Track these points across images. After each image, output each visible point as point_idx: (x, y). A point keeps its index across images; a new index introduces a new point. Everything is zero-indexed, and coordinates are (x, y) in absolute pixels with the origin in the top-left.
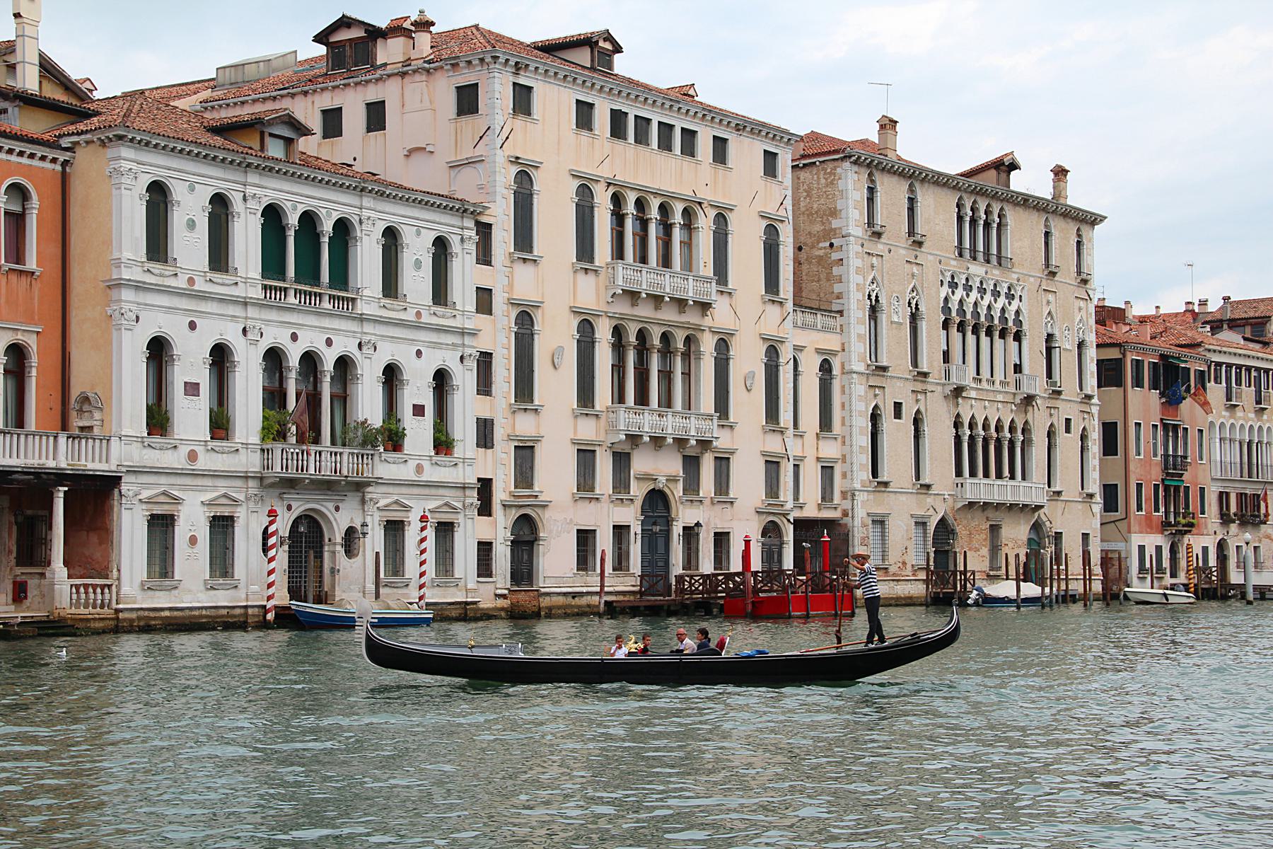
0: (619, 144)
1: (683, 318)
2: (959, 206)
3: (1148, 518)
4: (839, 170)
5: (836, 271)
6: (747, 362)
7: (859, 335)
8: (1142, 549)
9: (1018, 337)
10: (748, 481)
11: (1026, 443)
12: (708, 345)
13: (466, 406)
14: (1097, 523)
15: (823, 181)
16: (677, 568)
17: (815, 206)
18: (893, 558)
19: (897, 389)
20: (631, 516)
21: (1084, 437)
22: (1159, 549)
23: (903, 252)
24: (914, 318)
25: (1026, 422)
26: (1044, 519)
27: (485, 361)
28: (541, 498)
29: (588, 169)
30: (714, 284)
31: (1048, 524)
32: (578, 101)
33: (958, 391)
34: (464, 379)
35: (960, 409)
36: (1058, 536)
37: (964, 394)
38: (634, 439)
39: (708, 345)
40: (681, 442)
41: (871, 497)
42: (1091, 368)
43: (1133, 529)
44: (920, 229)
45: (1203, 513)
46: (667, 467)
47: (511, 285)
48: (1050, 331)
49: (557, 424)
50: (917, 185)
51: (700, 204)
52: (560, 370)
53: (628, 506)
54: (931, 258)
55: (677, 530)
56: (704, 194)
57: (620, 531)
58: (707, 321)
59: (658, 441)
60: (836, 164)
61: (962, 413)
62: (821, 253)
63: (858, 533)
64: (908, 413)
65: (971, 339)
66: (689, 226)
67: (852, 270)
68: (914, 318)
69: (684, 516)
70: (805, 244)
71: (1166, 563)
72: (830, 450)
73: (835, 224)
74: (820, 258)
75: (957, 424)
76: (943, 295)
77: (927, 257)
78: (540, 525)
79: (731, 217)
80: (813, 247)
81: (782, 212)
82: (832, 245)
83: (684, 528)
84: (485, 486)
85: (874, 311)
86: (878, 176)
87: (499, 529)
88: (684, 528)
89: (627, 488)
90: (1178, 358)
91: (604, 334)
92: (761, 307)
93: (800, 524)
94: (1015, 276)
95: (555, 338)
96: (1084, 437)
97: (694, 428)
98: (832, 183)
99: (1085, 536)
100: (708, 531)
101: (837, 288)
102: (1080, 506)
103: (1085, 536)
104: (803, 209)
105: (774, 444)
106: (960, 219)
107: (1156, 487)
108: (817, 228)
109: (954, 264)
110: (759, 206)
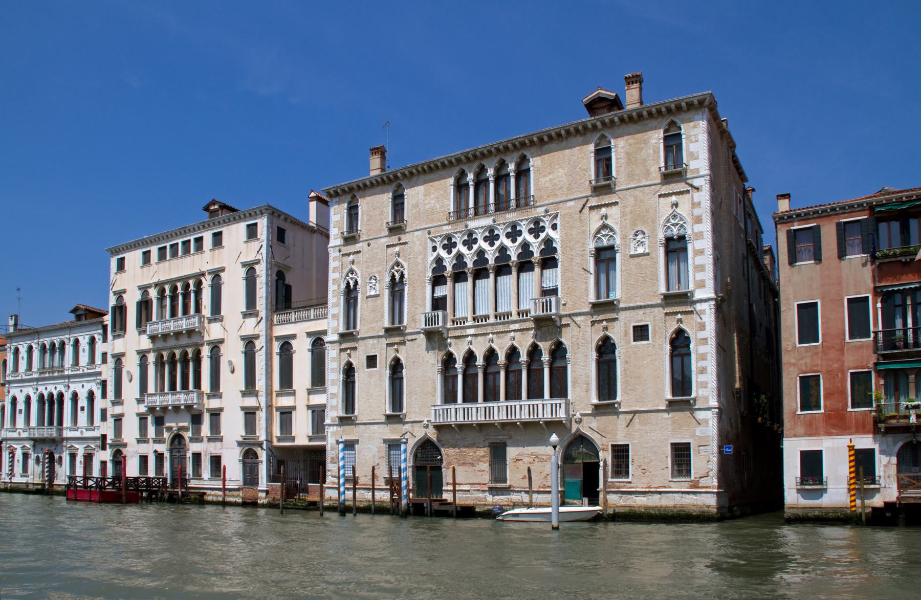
10: (233, 427)
12: (206, 351)
13: (99, 404)
20: (163, 448)
27: (104, 384)
34: (98, 393)
38: (165, 409)
39: (206, 351)
40: (189, 407)
54: (416, 233)
55: (189, 455)
57: (160, 457)
59: (177, 408)
68: (396, 287)
72: (318, 399)
75: (448, 361)
81: (259, 257)
83: (193, 454)
84: (104, 437)
87: (107, 455)
88: (193, 454)
91: (151, 358)
92: (242, 320)
94: (543, 209)
95: (131, 365)
105: (250, 402)
110: (244, 259)
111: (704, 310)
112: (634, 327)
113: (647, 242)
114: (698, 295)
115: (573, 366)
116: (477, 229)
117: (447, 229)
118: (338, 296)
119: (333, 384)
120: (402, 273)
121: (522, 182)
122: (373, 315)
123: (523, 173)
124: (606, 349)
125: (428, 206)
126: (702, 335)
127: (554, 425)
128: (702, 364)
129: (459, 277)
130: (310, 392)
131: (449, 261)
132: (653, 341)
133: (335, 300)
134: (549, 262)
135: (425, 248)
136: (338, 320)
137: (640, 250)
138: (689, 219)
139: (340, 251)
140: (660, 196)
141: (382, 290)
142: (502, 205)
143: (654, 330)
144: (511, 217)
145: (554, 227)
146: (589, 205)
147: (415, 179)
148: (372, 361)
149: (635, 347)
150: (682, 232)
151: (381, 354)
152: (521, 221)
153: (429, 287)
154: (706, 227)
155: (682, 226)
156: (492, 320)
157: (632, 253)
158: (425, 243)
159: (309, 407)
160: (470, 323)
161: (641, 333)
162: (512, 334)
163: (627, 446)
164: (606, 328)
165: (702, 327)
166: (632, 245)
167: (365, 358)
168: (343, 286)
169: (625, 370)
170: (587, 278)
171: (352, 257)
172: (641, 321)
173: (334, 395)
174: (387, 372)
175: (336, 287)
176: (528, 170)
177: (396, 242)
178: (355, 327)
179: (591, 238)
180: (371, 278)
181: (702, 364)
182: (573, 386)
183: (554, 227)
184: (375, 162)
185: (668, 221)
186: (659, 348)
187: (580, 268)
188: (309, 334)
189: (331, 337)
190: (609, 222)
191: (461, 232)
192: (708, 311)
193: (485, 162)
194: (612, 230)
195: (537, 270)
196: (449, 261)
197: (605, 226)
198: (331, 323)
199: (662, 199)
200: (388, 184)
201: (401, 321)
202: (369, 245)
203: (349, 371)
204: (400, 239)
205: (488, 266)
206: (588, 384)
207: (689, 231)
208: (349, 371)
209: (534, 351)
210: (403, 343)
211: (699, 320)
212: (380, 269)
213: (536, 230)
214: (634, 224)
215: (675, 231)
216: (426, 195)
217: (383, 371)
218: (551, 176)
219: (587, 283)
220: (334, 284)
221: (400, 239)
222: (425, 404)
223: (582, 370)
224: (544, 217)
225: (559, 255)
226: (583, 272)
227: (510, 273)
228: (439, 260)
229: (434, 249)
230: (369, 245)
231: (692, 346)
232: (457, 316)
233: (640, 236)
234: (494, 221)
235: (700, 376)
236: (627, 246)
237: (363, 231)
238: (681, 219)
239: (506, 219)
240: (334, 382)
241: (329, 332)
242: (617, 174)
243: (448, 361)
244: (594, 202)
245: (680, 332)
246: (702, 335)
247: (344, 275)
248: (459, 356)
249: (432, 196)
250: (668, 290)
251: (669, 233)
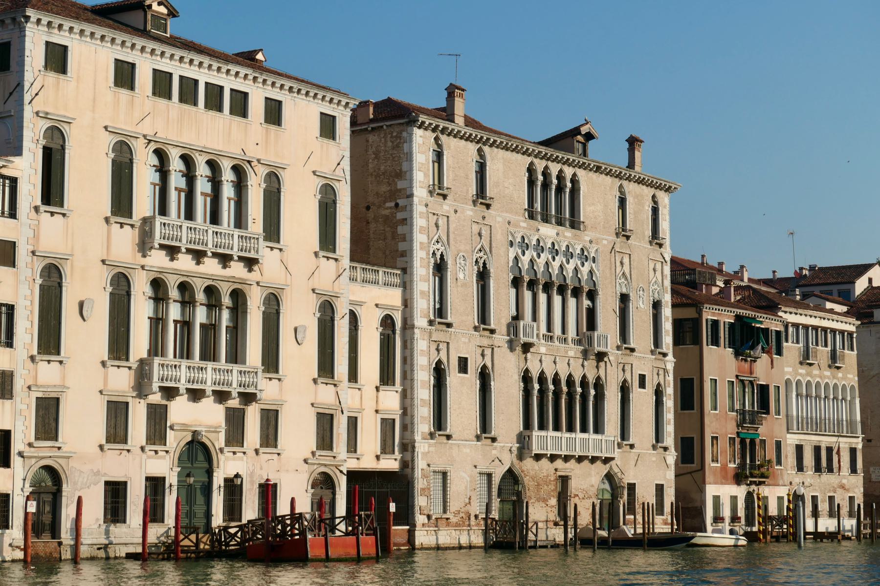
0: (162, 102)
1: (228, 272)
2: (531, 170)
3: (724, 468)
4: (404, 134)
5: (400, 230)
6: (299, 316)
7: (422, 292)
8: (717, 499)
9: (592, 295)
10: (298, 435)
11: (600, 397)
14: (671, 475)
15: (389, 144)
16: (218, 520)
17: (382, 168)
18: (454, 505)
19: (464, 342)
20: (165, 465)
21: (659, 393)
22: (734, 499)
24: (483, 276)
25: (598, 378)
26: (616, 470)
28: (64, 449)
29: (125, 125)
30: (261, 240)
31: (619, 474)
32: (116, 59)
33: (527, 347)
35: (529, 365)
36: (632, 487)
37: (531, 350)
41: (432, 449)
42: (667, 326)
43: (707, 480)
44: (489, 193)
45: (779, 462)
46: (208, 417)
47: (36, 236)
48: (624, 291)
49: (85, 375)
50: (486, 149)
51: (249, 162)
52: (89, 322)
53: (163, 458)
55: (218, 480)
56: (253, 153)
58: (254, 276)
60: (402, 128)
61: (530, 368)
62: (387, 212)
63: (420, 483)
65: (542, 298)
66: (240, 185)
67: (416, 229)
68: (483, 276)
69: (227, 466)
70: (374, 204)
71: (741, 513)
73: (400, 184)
74: (387, 219)
75: (526, 378)
76: (512, 256)
77: (497, 216)
78: (63, 477)
79: (286, 177)
80: (379, 207)
81: (339, 172)
82: (397, 205)
85: (440, 268)
86: (444, 138)
89: (163, 440)
90: (754, 319)
93: (353, 476)
96: (659, 393)
97: (235, 381)
98: (398, 146)
99: (660, 489)
100: (252, 482)
101: (402, 246)
103: (660, 489)
104: (371, 170)
105: (326, 395)
106: (531, 183)
107: (732, 440)
108: (384, 188)
109: (523, 226)
110: (313, 165)
139: (427, 205)
144: (568, 233)
193: (550, 164)
221: (484, 218)
230: (456, 211)
234: (558, 234)
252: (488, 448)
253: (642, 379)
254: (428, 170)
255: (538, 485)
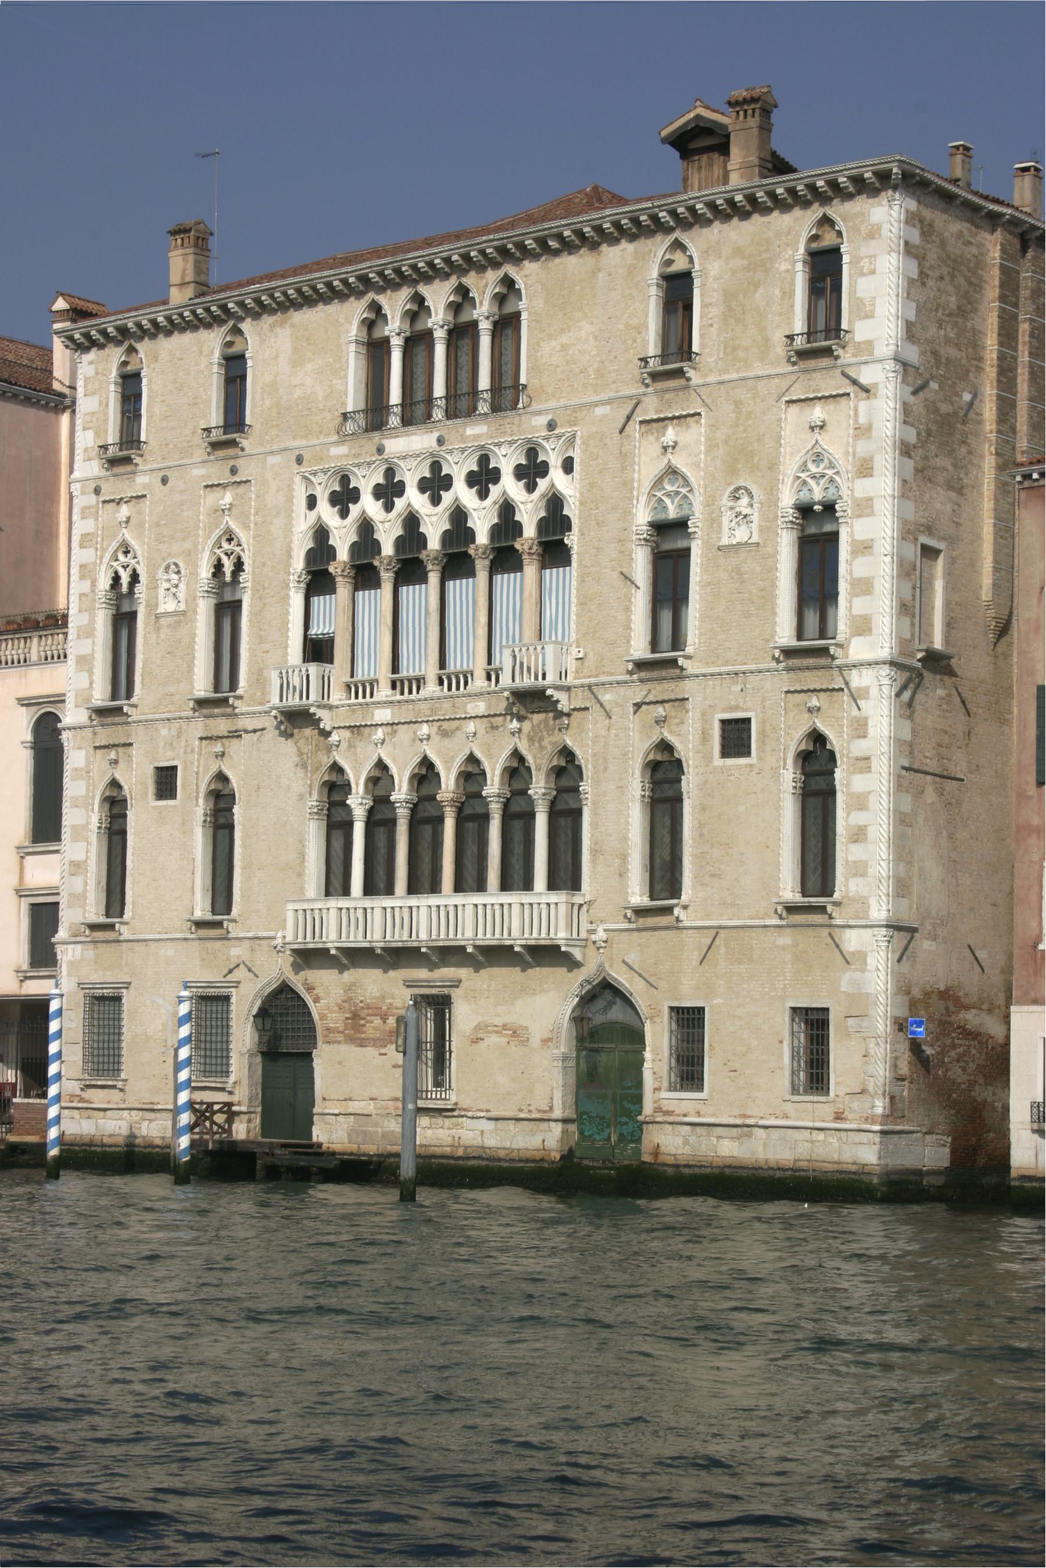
21: (817, 760)
23: (199, 472)
54: (272, 460)
64: (195, 788)
75: (335, 788)
94: (542, 420)
96: (817, 760)
102: (785, 939)
106: (376, 350)
111: (868, 688)
112: (723, 722)
113: (755, 517)
114: (858, 650)
115: (594, 813)
116: (404, 458)
117: (339, 453)
118: (91, 610)
119: (74, 839)
120: (239, 558)
121: (508, 344)
122: (177, 658)
123: (507, 325)
124: (664, 772)
125: (298, 393)
126: (860, 747)
127: (546, 954)
128: (859, 818)
129: (365, 575)
130: (23, 854)
131: (343, 538)
132: (759, 758)
133: (85, 619)
134: (554, 552)
135: (290, 500)
136: (91, 672)
137: (741, 535)
138: (845, 464)
139: (97, 491)
140: (790, 402)
141: (191, 600)
142: (461, 403)
143: (762, 733)
145: (568, 466)
146: (638, 417)
147: (267, 320)
148: (166, 782)
149: (723, 770)
150: (831, 495)
151: (185, 769)
152: (499, 445)
153: (297, 600)
154: (883, 485)
155: (832, 480)
156: (431, 688)
157: (725, 541)
158: (290, 487)
159: (20, 893)
160: (384, 692)
161: (736, 737)
162: (471, 726)
163: (701, 1010)
164: (660, 722)
165: (860, 728)
166: (725, 520)
167: (150, 772)
168: (104, 582)
169: (701, 826)
170: (628, 598)
171: (125, 511)
172: (736, 708)
173: (77, 867)
174: (200, 809)
175: (86, 587)
176: (517, 315)
177: (226, 478)
178: (129, 695)
179: (643, 499)
180: (167, 568)
181: (859, 818)
182: (594, 861)
183: (568, 466)
184: (180, 263)
185: (804, 468)
186: (772, 780)
187: (616, 575)
188: (25, 702)
189: (72, 716)
190: (679, 461)
191: (369, 464)
192: (874, 692)
193: (423, 289)
194: (686, 482)
195: (530, 570)
196: (343, 538)
197: (672, 472)
198: (77, 677)
199: (794, 409)
200: (208, 326)
201: (234, 685)
202: (164, 481)
203: (115, 805)
204: (234, 471)
205: (423, 556)
206: (624, 858)
207: (844, 492)
208: (115, 805)
209: (517, 770)
210: (235, 735)
211: (855, 712)
212: (188, 545)
213: (531, 471)
214: (732, 470)
215: (817, 493)
216: (297, 362)
217: (192, 804)
218: (564, 339)
219: (628, 609)
220: (82, 577)
221: (234, 471)
222: (288, 897)
223: (615, 820)
224: (547, 439)
225: (572, 540)
226: (619, 582)
227: (471, 573)
228: (321, 534)
229: (312, 502)
230: (164, 481)
231: (838, 774)
232: (359, 676)
233: (745, 500)
234: (440, 441)
235: (853, 847)
236: (714, 523)
237: (153, 443)
238: (831, 466)
239: (463, 438)
240: (79, 833)
241: (70, 699)
242: (702, 345)
243: (335, 788)
244: (650, 409)
245: (818, 738)
246: (860, 747)
247: (108, 556)
248: (358, 781)
249: (309, 367)
250: (800, 636)
251: (804, 497)
252: (218, 944)
253: (736, 737)
254: (106, 421)
255: (355, 1016)
